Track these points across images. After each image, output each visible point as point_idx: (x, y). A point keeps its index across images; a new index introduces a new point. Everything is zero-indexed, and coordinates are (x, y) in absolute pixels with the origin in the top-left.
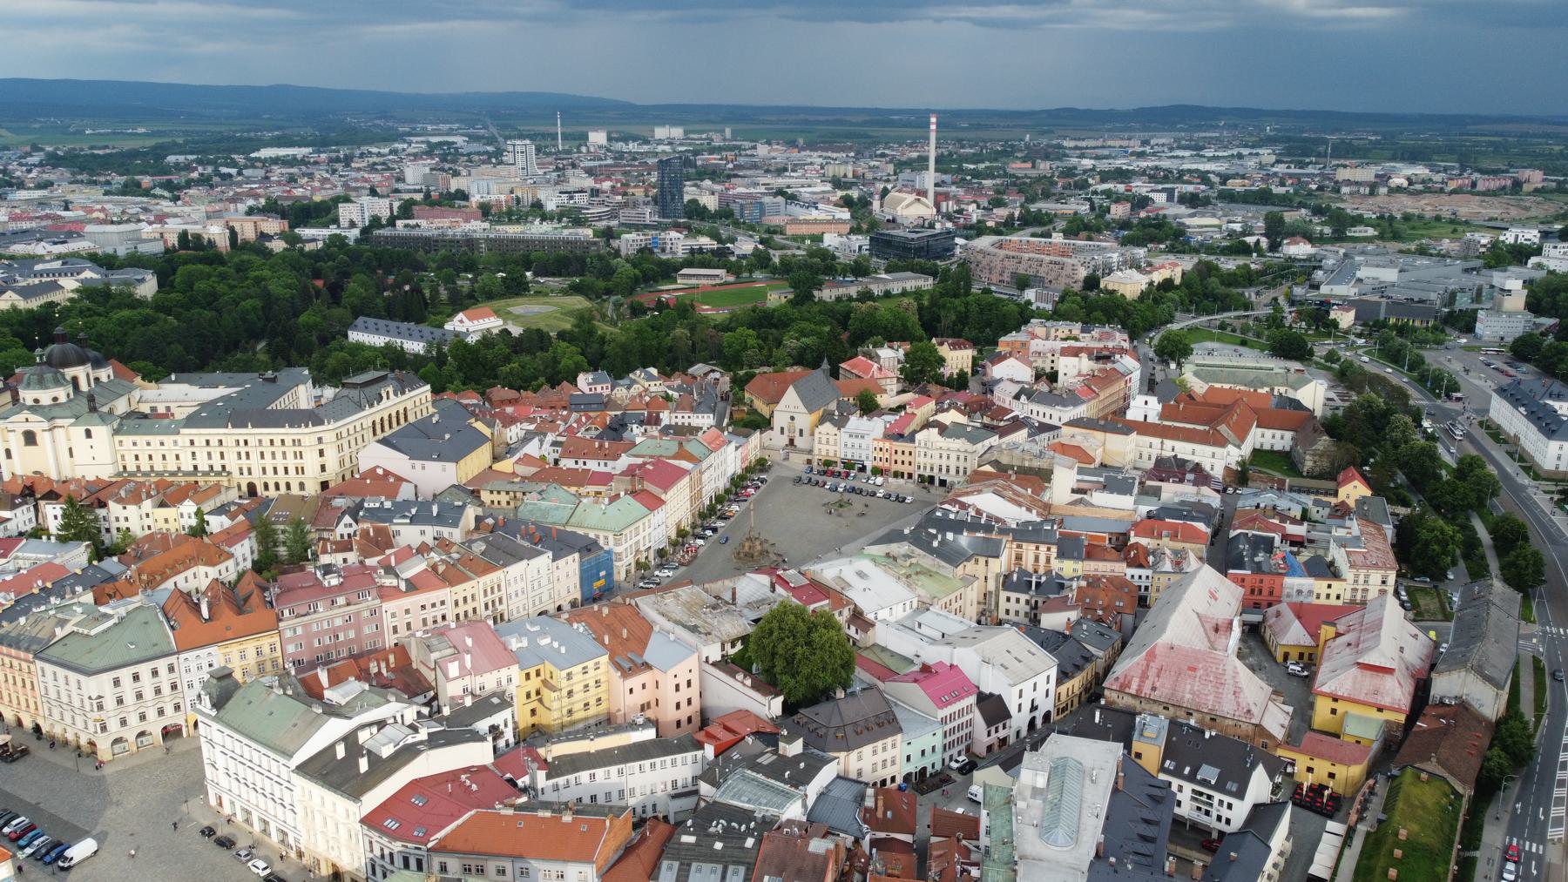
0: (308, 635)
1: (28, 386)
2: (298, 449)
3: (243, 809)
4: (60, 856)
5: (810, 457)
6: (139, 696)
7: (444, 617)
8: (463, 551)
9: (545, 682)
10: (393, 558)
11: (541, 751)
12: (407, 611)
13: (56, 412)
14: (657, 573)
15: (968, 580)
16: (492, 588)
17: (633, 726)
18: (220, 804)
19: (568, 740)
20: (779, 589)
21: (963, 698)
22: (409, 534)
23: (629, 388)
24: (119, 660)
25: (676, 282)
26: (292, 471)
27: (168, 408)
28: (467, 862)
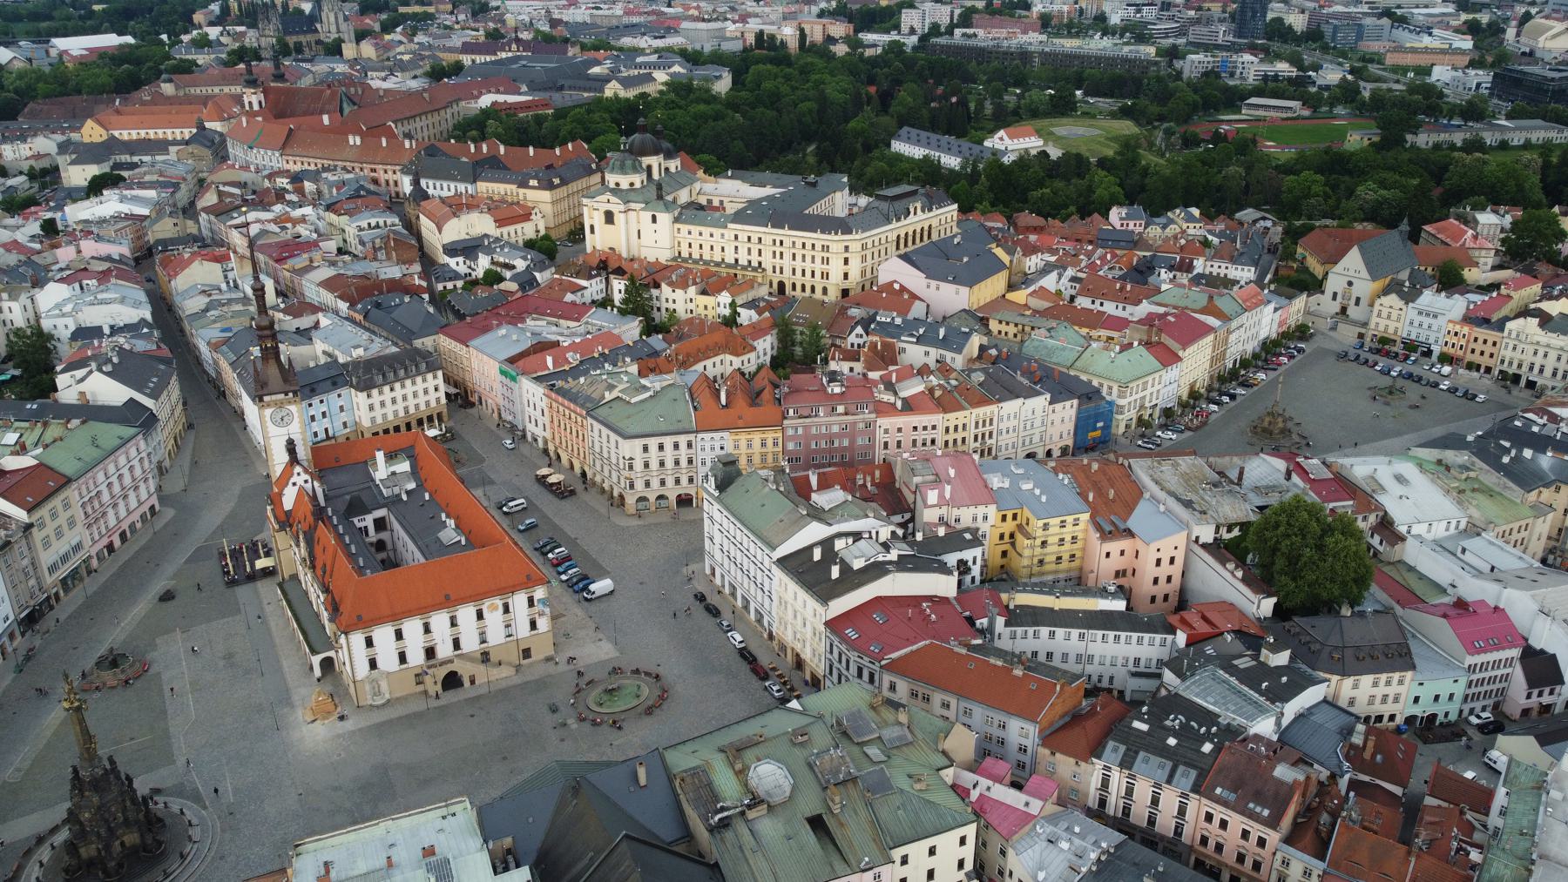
0: (807, 436)
1: (612, 171)
2: (826, 255)
3: (730, 584)
4: (585, 588)
5: (1363, 331)
6: (662, 464)
7: (933, 442)
8: (961, 379)
9: (1020, 527)
10: (894, 375)
11: (1004, 596)
12: (900, 430)
13: (632, 196)
14: (1159, 433)
15: (1541, 510)
16: (984, 421)
17: (1103, 593)
18: (713, 574)
19: (1033, 591)
20: (1295, 478)
21: (1503, 648)
22: (914, 353)
23: (1164, 227)
24: (648, 430)
25: (1240, 113)
26: (818, 275)
27: (721, 202)
28: (915, 688)
